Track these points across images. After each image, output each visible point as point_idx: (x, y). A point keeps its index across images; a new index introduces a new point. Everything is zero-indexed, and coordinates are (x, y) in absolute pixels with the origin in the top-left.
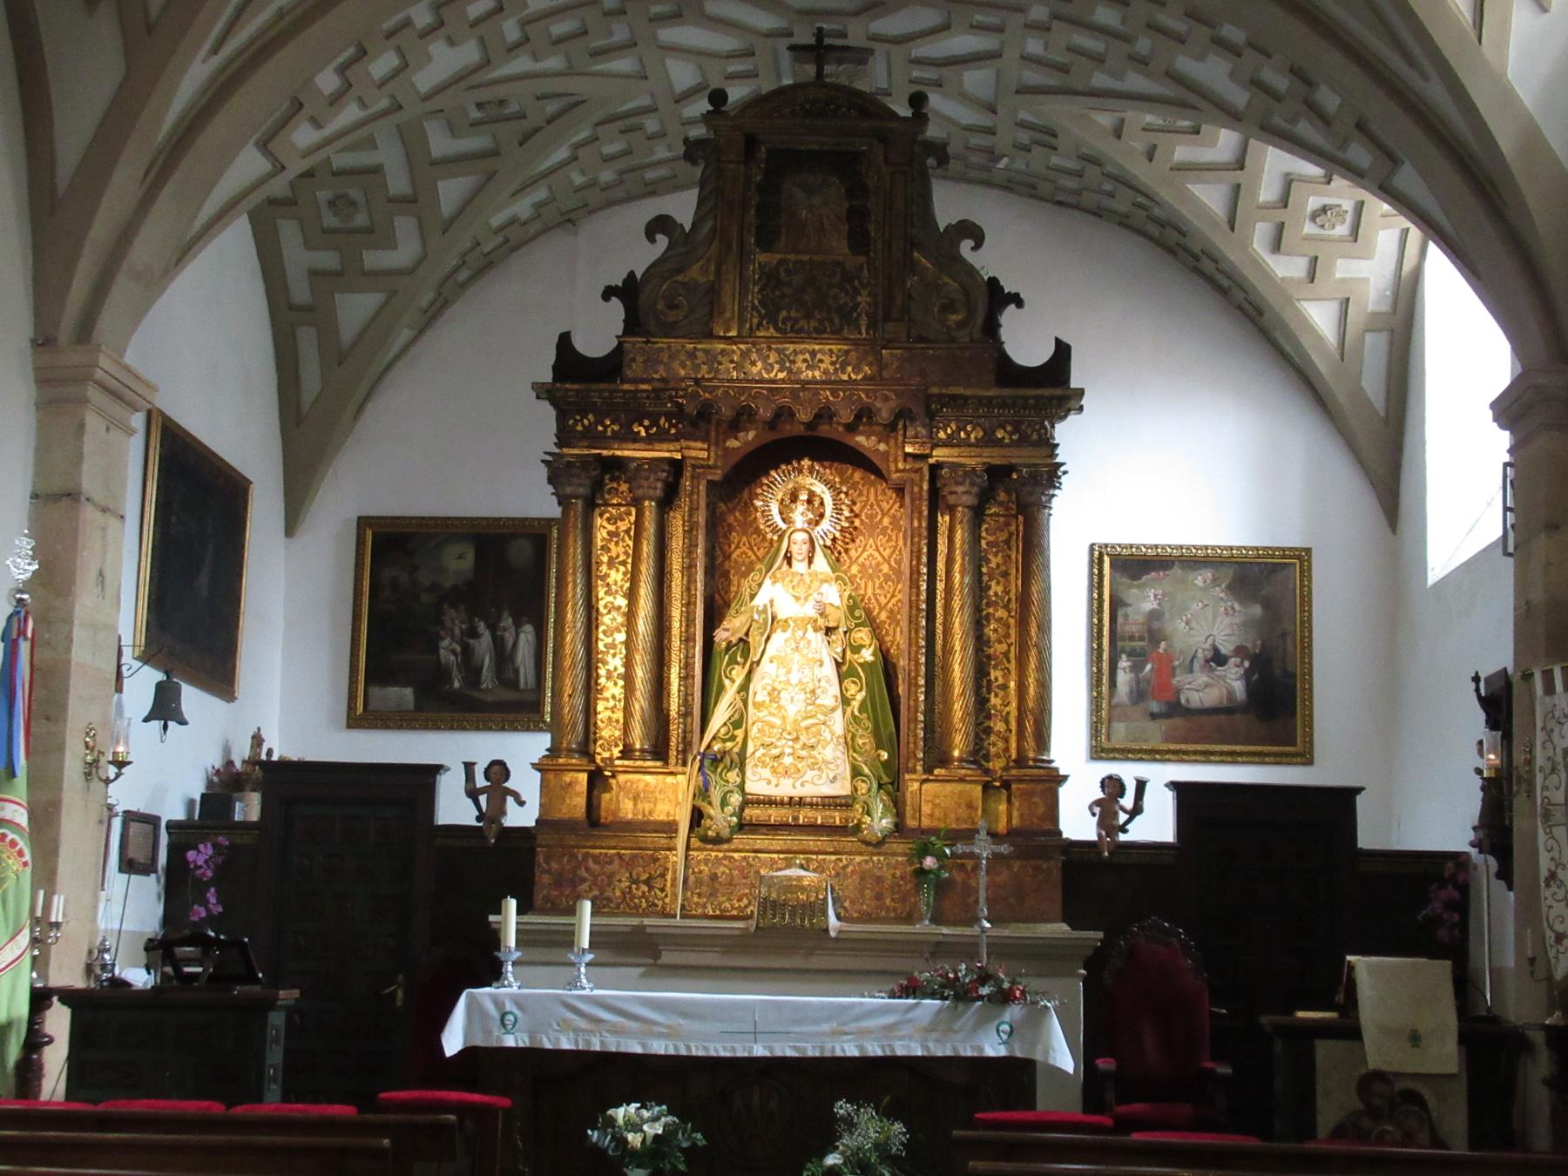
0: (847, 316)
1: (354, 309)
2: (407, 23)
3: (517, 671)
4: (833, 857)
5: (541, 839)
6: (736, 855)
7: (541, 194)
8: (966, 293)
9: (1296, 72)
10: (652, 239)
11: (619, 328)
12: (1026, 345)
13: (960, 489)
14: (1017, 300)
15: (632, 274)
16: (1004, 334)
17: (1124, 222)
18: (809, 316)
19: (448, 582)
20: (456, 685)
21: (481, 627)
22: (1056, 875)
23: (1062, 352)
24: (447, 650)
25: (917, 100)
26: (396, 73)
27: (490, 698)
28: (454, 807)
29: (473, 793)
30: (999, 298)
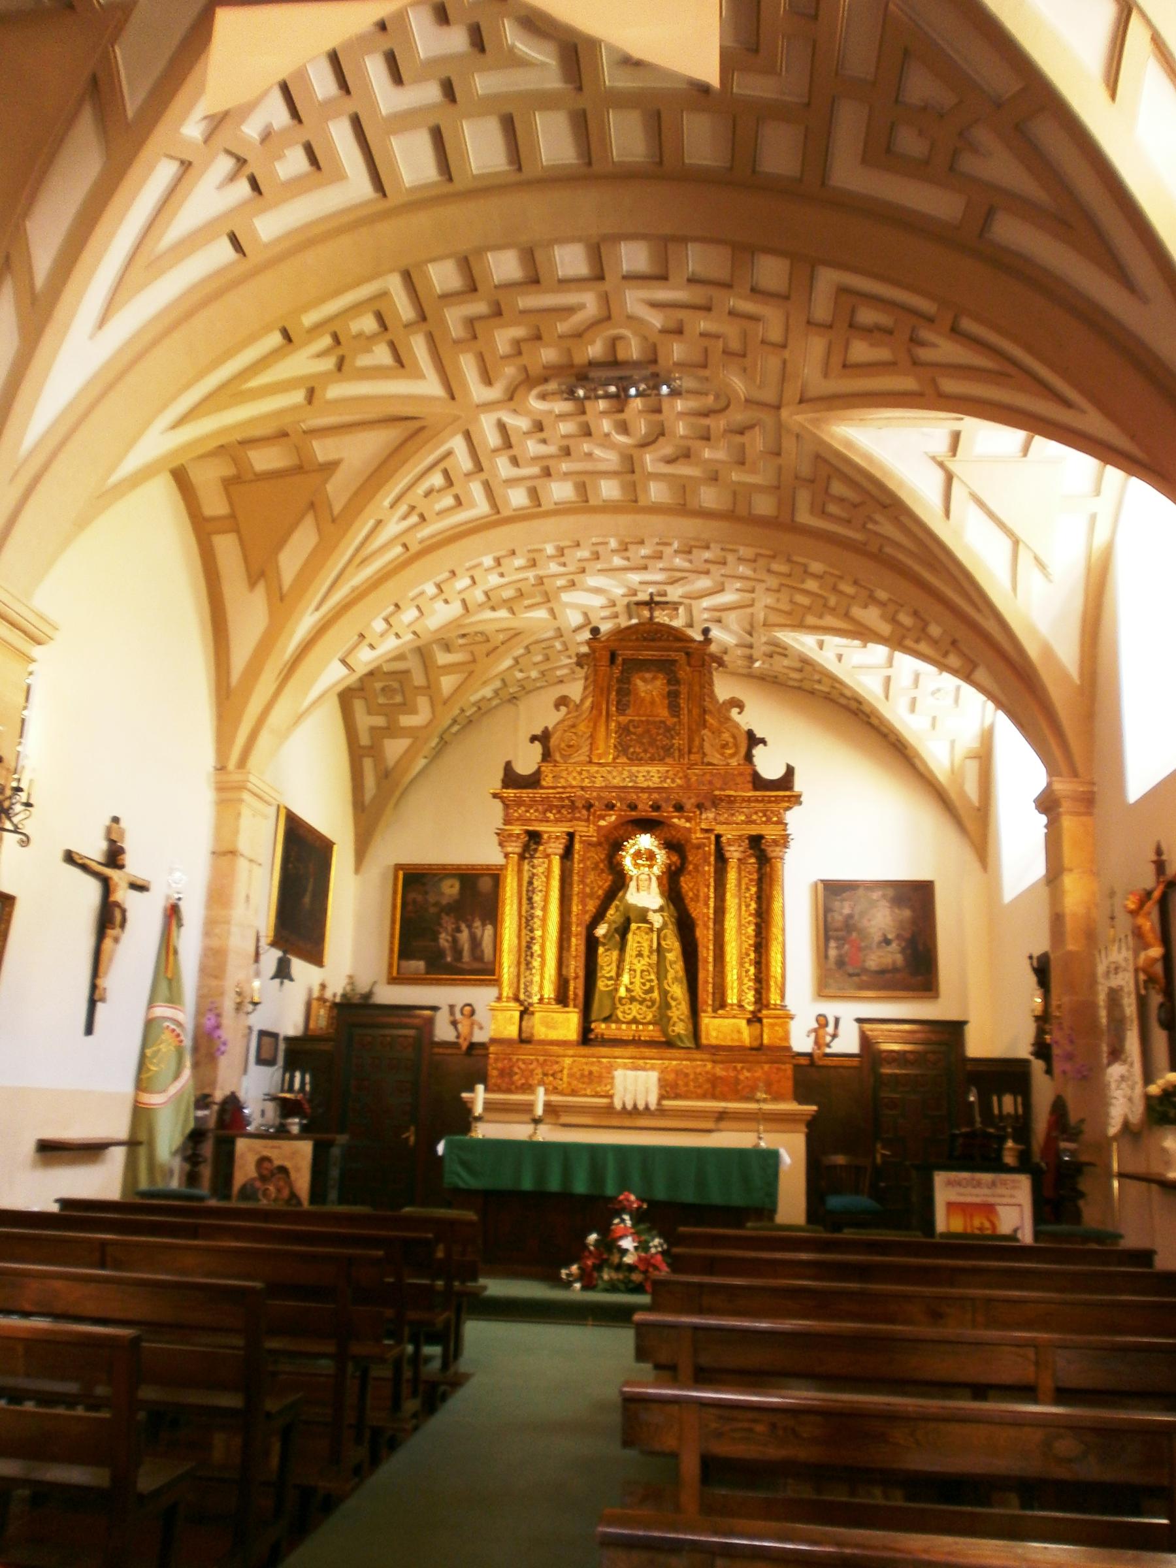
0: (668, 751)
1: (394, 748)
2: (422, 593)
3: (482, 952)
4: (660, 1062)
5: (492, 1049)
6: (604, 1060)
7: (498, 684)
8: (734, 737)
9: (916, 613)
10: (557, 706)
11: (539, 758)
12: (769, 765)
13: (732, 848)
14: (763, 741)
15: (546, 728)
16: (756, 760)
17: (828, 698)
18: (645, 751)
19: (444, 902)
20: (449, 959)
21: (463, 927)
22: (790, 1073)
23: (790, 771)
24: (444, 940)
25: (706, 631)
26: (417, 619)
27: (465, 966)
28: (444, 1032)
29: (454, 1023)
30: (753, 740)
